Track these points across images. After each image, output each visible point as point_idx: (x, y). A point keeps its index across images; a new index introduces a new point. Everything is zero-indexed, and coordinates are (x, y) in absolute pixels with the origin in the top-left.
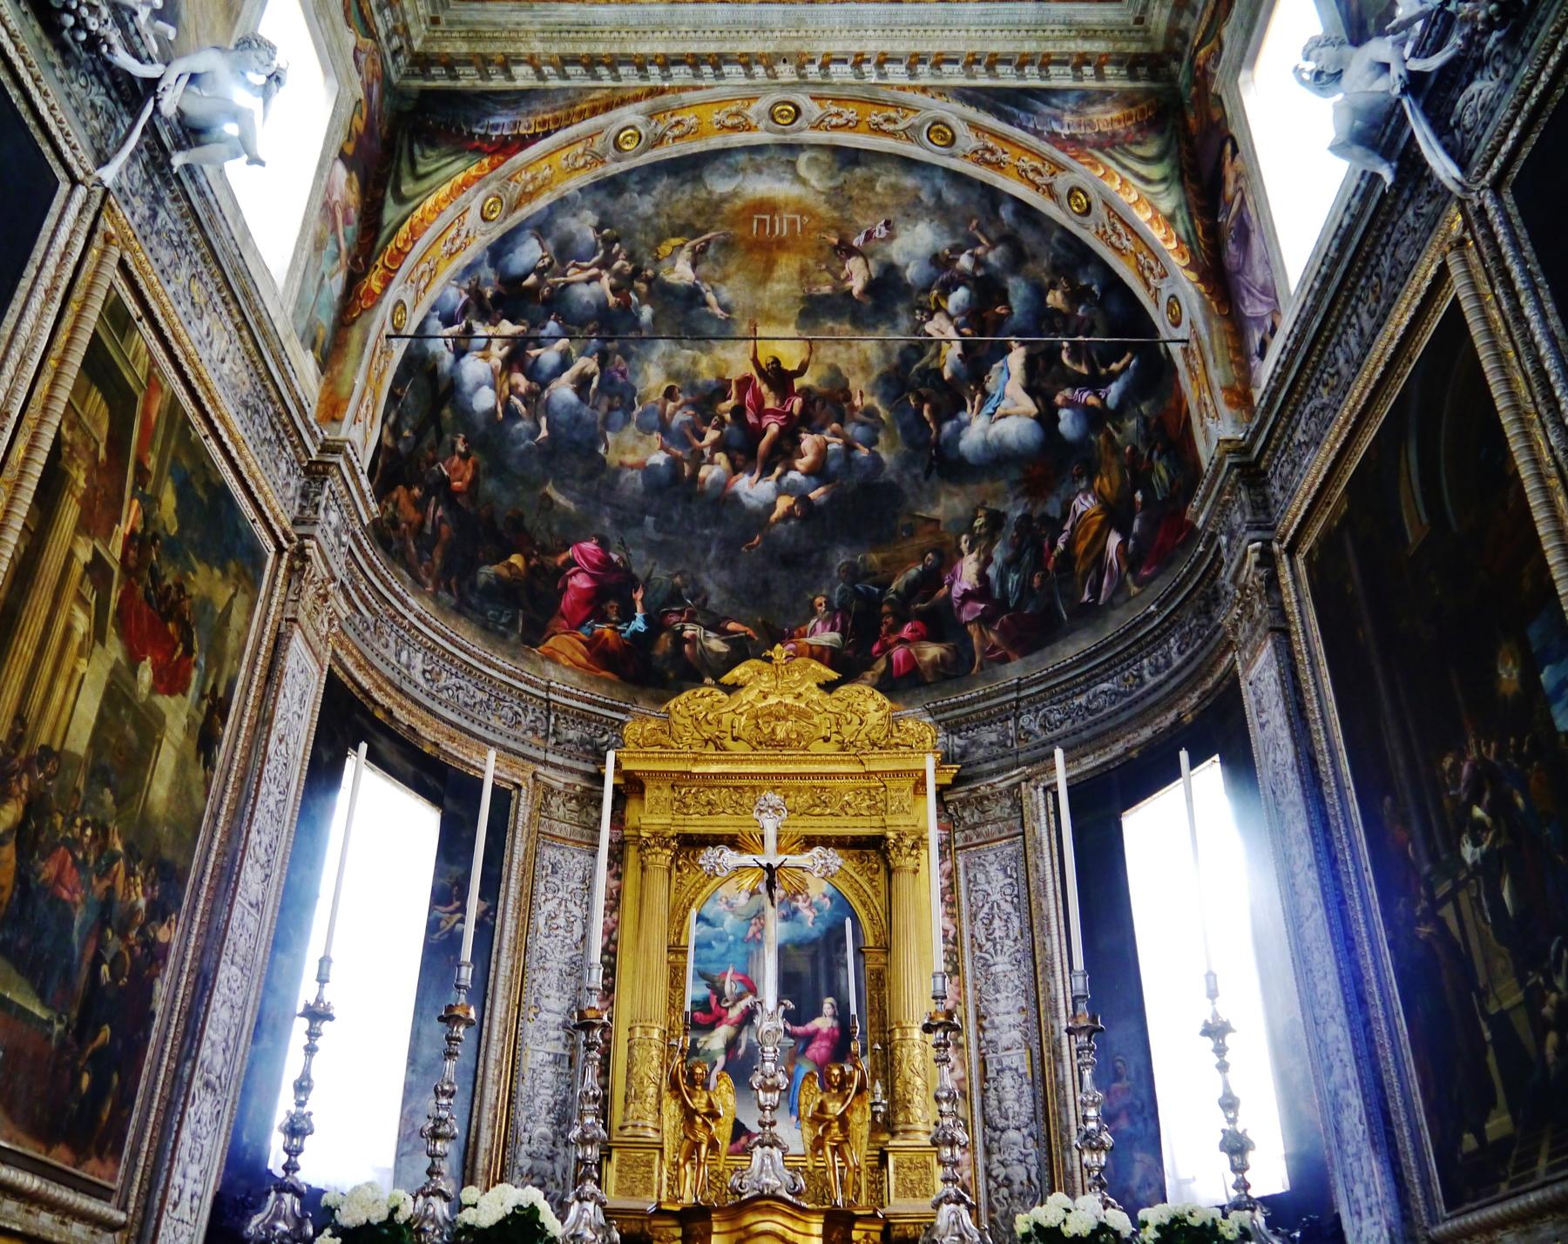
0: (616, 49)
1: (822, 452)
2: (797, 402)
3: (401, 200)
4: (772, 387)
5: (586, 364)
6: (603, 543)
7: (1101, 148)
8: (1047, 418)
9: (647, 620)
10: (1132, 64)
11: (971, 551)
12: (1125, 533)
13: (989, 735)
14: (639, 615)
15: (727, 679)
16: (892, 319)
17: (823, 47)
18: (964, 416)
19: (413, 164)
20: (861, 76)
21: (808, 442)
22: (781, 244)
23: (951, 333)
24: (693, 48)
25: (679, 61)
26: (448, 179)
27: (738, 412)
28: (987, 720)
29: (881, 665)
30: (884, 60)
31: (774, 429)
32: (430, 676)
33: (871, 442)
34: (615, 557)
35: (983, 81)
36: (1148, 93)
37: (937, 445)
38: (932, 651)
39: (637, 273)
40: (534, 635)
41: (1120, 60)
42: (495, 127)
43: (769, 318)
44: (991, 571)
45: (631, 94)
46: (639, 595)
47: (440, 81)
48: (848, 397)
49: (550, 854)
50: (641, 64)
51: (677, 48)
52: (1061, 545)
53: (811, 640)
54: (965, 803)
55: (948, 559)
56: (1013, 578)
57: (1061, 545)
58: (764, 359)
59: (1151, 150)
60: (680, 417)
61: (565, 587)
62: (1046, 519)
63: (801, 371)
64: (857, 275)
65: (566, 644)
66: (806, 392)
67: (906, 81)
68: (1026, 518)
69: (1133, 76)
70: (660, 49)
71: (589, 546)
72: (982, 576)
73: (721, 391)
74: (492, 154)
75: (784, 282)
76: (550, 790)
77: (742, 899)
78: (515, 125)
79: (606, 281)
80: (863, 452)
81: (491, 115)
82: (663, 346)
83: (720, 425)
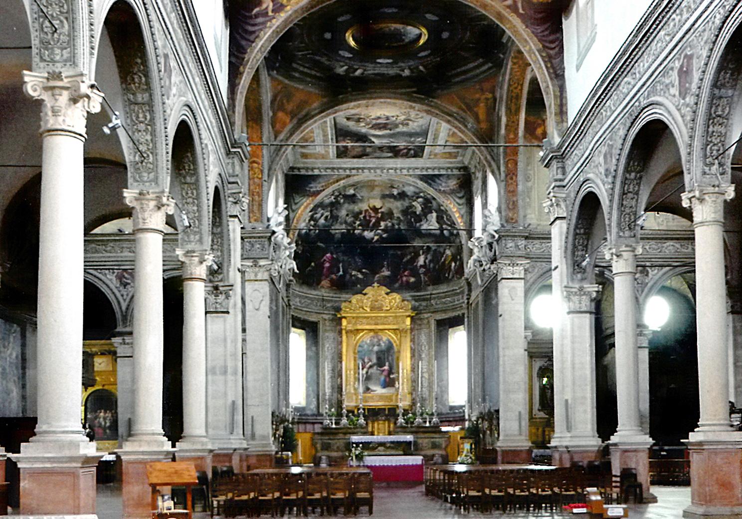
0: (339, 166)
1: (386, 226)
2: (380, 215)
3: (293, 211)
4: (373, 211)
5: (328, 213)
6: (332, 254)
7: (449, 194)
8: (441, 229)
9: (343, 271)
10: (459, 169)
11: (423, 253)
12: (455, 263)
13: (424, 304)
14: (341, 270)
15: (364, 292)
16: (404, 200)
17: (388, 166)
18: (422, 223)
19: (294, 199)
20: (396, 172)
21: (382, 224)
22: (377, 186)
23: (419, 205)
24: (357, 166)
25: (354, 169)
26: (302, 204)
27: (365, 217)
28: (424, 300)
29: (400, 282)
30: (401, 169)
31: (374, 220)
32: (300, 302)
33: (399, 224)
34: (335, 256)
35: (425, 173)
36: (463, 175)
37: (415, 227)
38: (412, 280)
39: (340, 194)
40: (318, 283)
41: (457, 168)
42: (311, 188)
43: (373, 198)
44: (427, 261)
45: (342, 177)
46: (341, 265)
47: (296, 172)
48: (393, 214)
49: (327, 334)
50: (345, 169)
51: (353, 166)
52: (443, 260)
53: (383, 274)
54: (418, 319)
55: (417, 255)
56: (432, 265)
57: (443, 260)
58: (371, 206)
59: (460, 195)
60: (350, 220)
61: (324, 268)
62: (440, 252)
63: (381, 208)
64: (395, 192)
65: (325, 283)
66: (382, 213)
67: (407, 173)
68: (435, 250)
69: (460, 171)
70: (349, 166)
71: (328, 255)
72: (425, 262)
73: (361, 213)
74: (312, 196)
75: (377, 192)
76: (325, 320)
77: (368, 342)
78: (316, 187)
79: (333, 197)
80: (397, 227)
81: (310, 184)
82: (346, 205)
83: (360, 220)
